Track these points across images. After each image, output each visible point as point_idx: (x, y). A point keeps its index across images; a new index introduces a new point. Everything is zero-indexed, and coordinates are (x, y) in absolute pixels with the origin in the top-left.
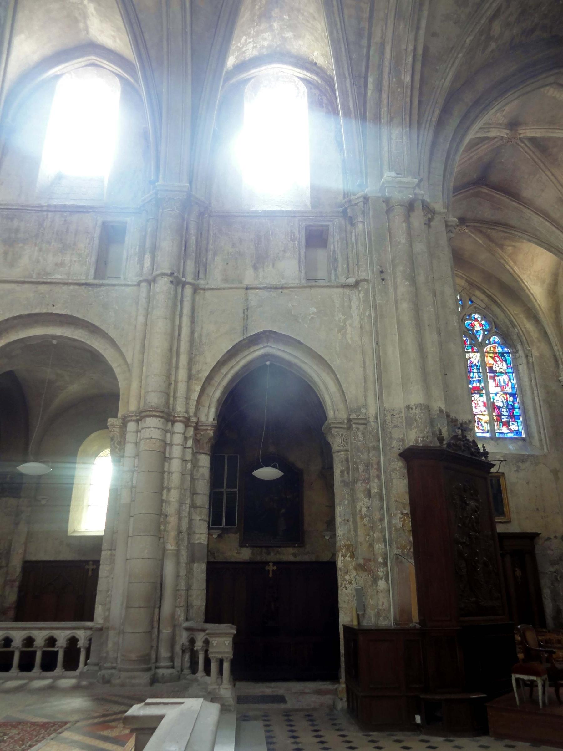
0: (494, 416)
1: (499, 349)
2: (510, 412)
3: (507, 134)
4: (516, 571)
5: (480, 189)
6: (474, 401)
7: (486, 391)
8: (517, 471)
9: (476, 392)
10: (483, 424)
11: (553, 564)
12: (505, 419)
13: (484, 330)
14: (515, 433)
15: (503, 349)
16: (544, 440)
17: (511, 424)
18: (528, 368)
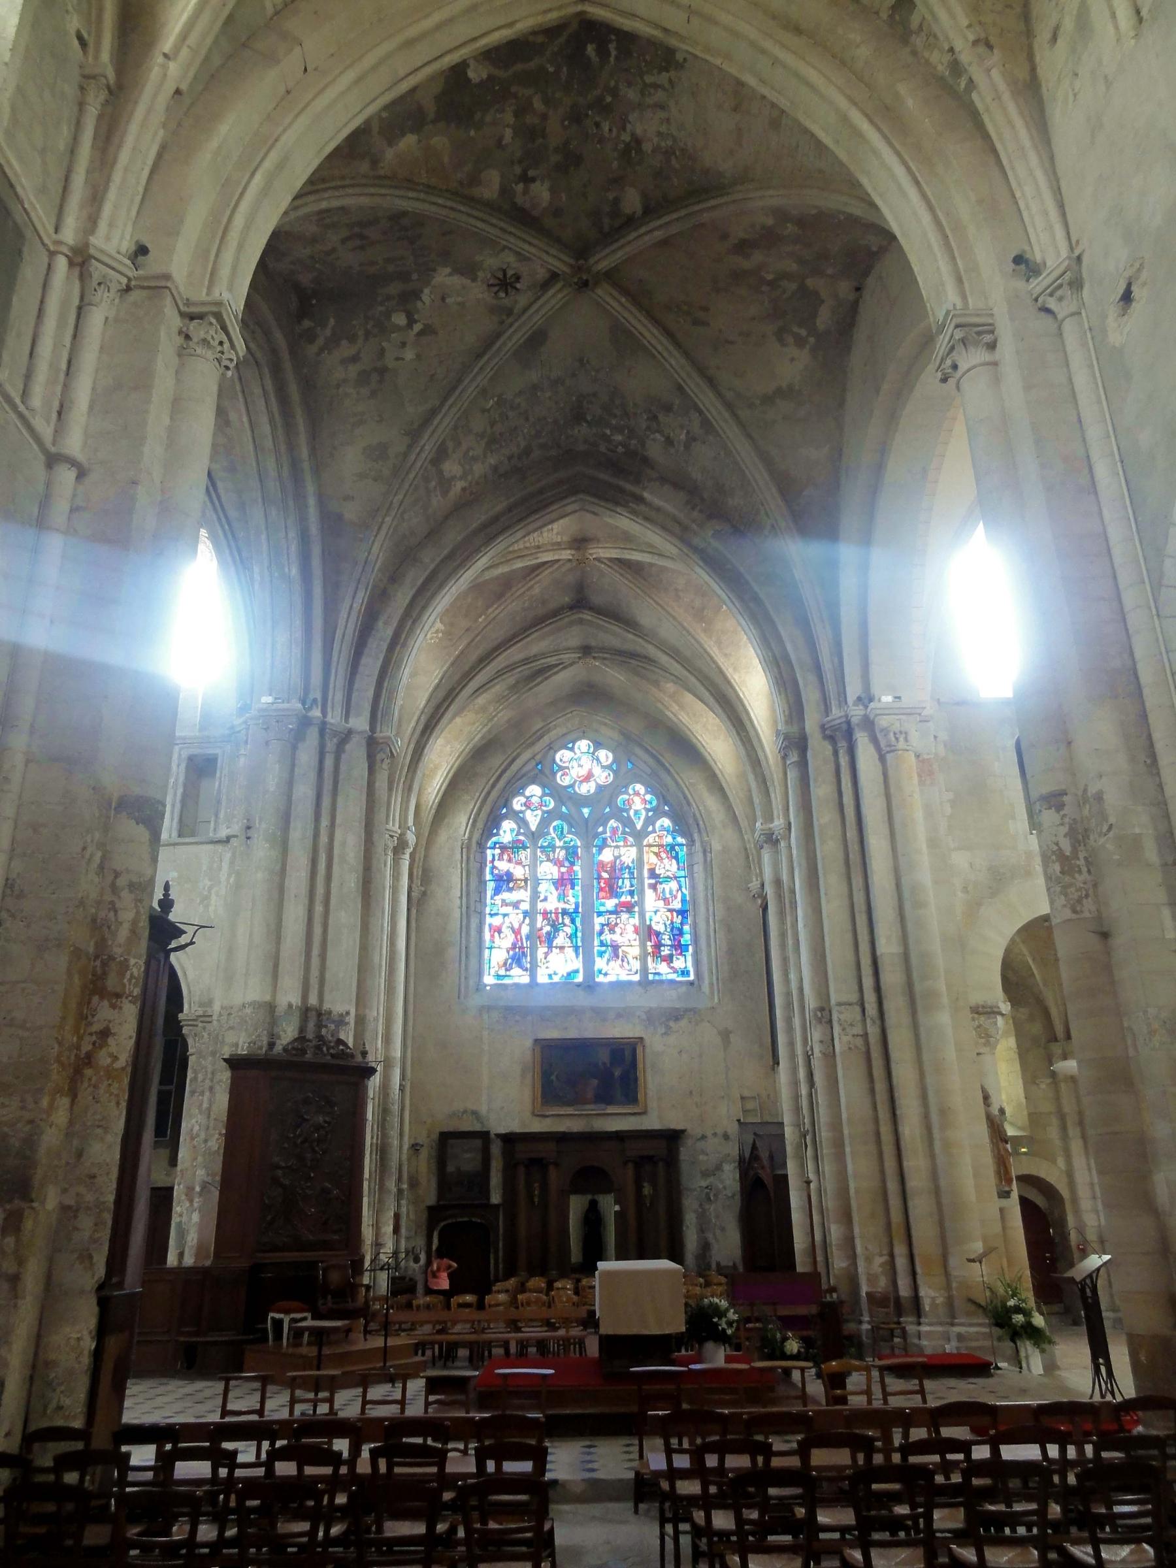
1: (669, 840)
3: (573, 555)
5: (581, 615)
11: (705, 1174)
12: (666, 951)
13: (648, 810)
15: (674, 838)
17: (674, 959)
18: (705, 869)
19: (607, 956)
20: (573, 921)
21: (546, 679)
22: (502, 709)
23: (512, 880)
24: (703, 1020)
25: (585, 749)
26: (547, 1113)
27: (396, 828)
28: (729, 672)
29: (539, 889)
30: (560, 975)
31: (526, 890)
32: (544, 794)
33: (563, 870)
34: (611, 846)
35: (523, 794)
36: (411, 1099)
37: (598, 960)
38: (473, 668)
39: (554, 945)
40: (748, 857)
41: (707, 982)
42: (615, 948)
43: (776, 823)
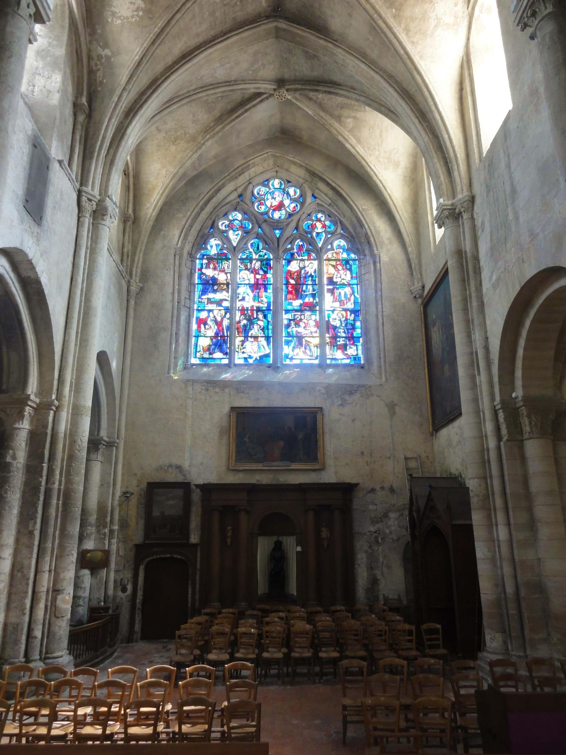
0: (327, 339)
1: (345, 256)
2: (348, 332)
4: (322, 531)
6: (304, 321)
7: (320, 308)
8: (342, 405)
9: (308, 308)
10: (312, 348)
11: (374, 521)
12: (341, 342)
14: (352, 359)
15: (348, 255)
17: (348, 348)
19: (292, 344)
20: (265, 317)
21: (246, 111)
22: (209, 139)
23: (217, 284)
24: (372, 395)
25: (277, 185)
26: (241, 468)
27: (96, 192)
28: (416, 59)
29: (238, 291)
31: (228, 292)
33: (258, 277)
34: (297, 260)
38: (176, 63)
39: (250, 335)
42: (300, 338)
43: (460, 196)
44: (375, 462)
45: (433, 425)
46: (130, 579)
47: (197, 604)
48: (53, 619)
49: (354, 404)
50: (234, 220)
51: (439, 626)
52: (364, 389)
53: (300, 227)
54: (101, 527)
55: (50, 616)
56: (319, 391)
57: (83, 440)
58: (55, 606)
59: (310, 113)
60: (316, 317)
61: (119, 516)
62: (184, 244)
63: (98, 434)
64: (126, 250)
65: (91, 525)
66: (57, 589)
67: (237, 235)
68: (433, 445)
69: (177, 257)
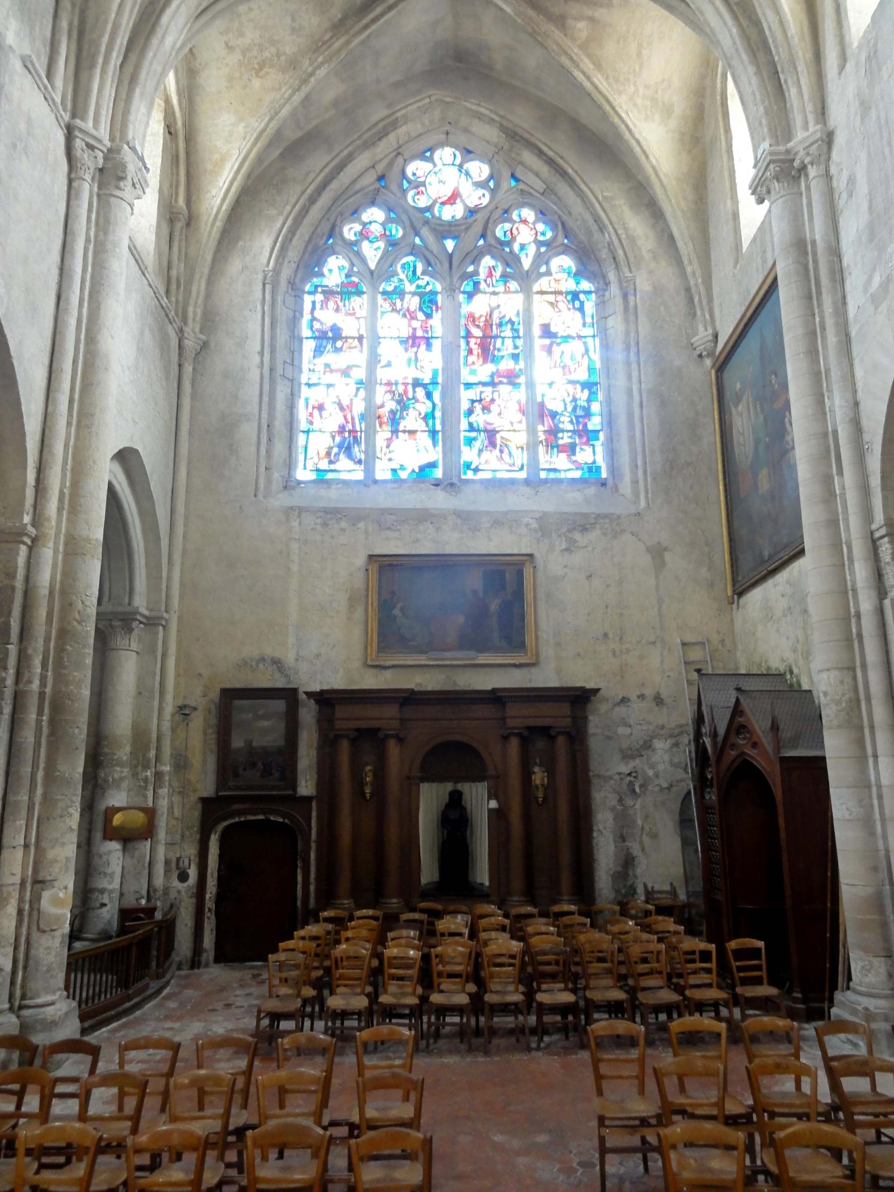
2: (578, 423)
4: (535, 773)
9: (505, 380)
11: (627, 755)
12: (565, 439)
13: (539, 244)
14: (586, 469)
16: (641, 482)
17: (578, 449)
19: (477, 445)
20: (429, 395)
22: (322, 63)
23: (341, 338)
24: (623, 531)
26: (387, 664)
27: (103, 133)
30: (409, 471)
32: (389, 220)
34: (485, 293)
35: (359, 220)
36: (179, 642)
37: (465, 449)
39: (401, 428)
40: (691, 300)
41: (627, 479)
42: (491, 434)
44: (628, 651)
45: (734, 585)
46: (193, 858)
47: (312, 900)
48: (35, 935)
49: (590, 549)
50: (370, 223)
51: (761, 944)
52: (607, 521)
53: (489, 233)
54: (140, 768)
55: (29, 928)
56: (527, 525)
57: (88, 603)
58: (39, 910)
59: (509, 10)
60: (521, 394)
61: (173, 747)
62: (281, 264)
63: (129, 604)
64: (174, 273)
65: (121, 765)
66: (40, 879)
67: (376, 249)
68: (732, 620)
69: (268, 288)
